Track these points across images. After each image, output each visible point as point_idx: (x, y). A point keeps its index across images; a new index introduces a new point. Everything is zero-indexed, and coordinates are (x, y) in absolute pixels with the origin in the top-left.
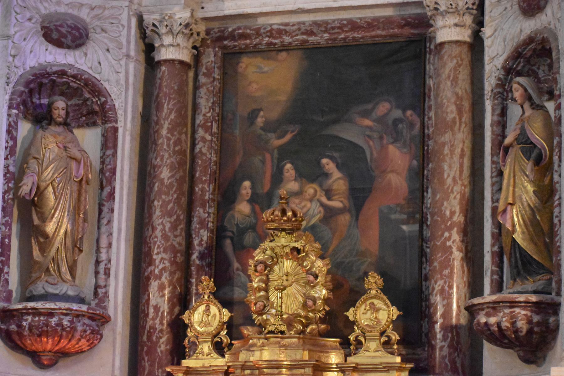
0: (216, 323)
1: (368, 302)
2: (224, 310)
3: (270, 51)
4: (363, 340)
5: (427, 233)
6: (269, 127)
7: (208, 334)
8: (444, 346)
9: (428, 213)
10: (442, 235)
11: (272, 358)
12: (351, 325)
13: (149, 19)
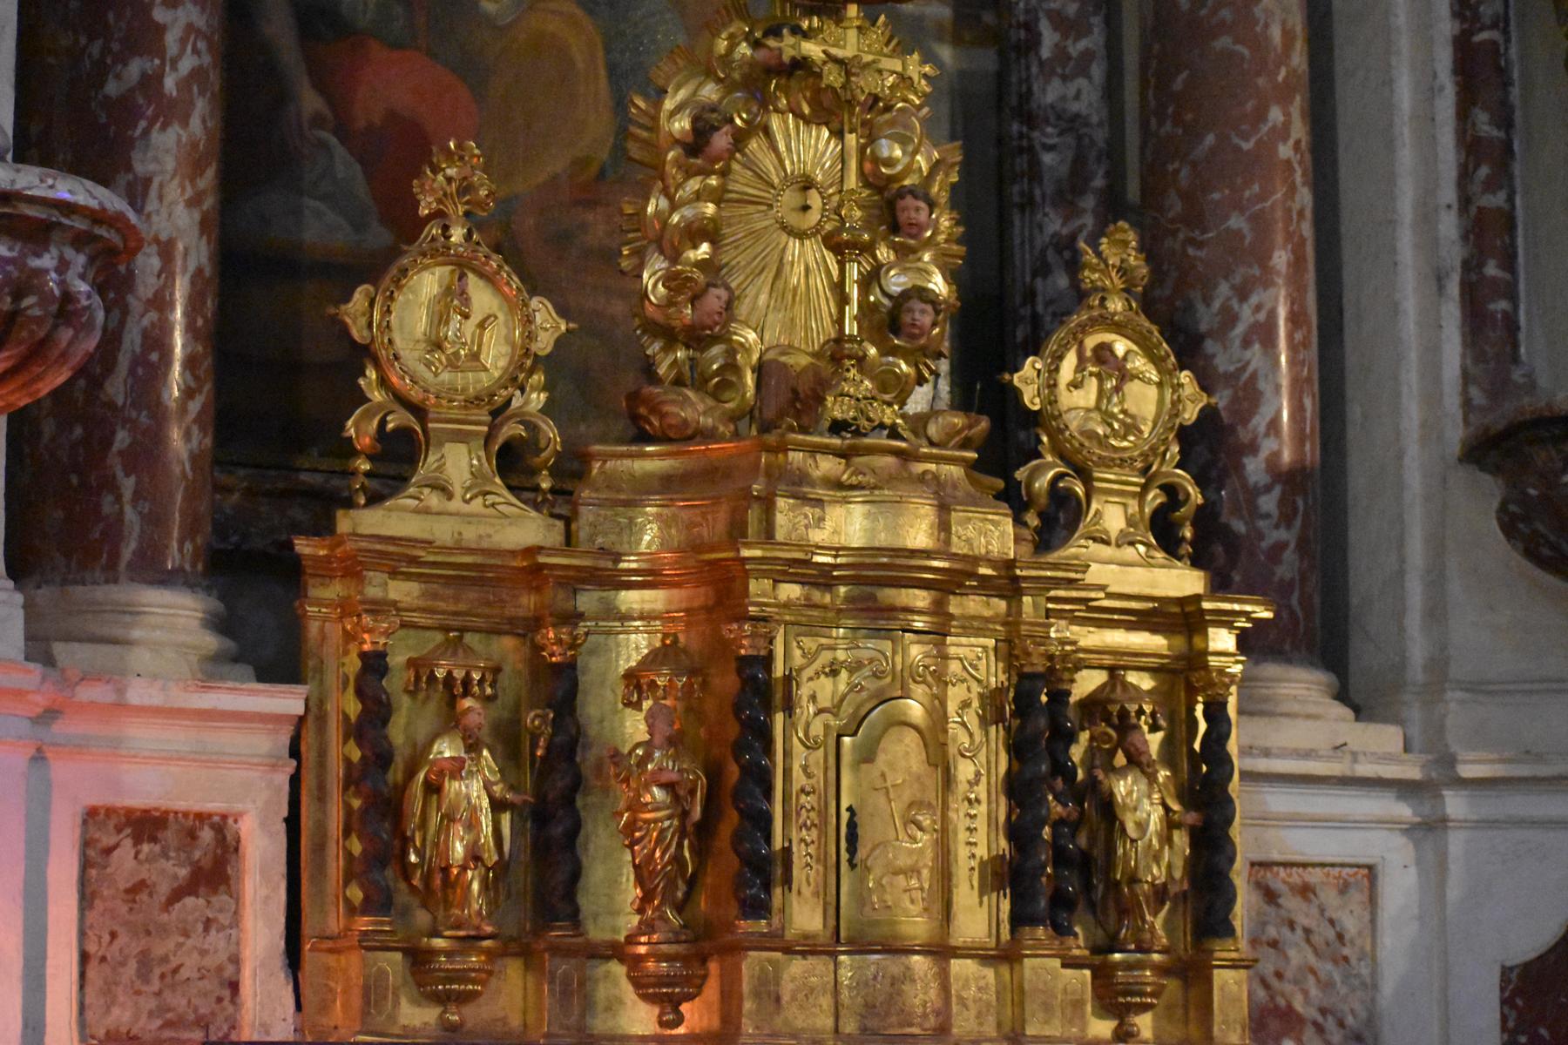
0: (496, 356)
1: (1091, 342)
2: (535, 302)
4: (1079, 490)
7: (475, 401)
8: (1280, 547)
9: (1041, 15)
10: (1261, 115)
11: (883, 540)
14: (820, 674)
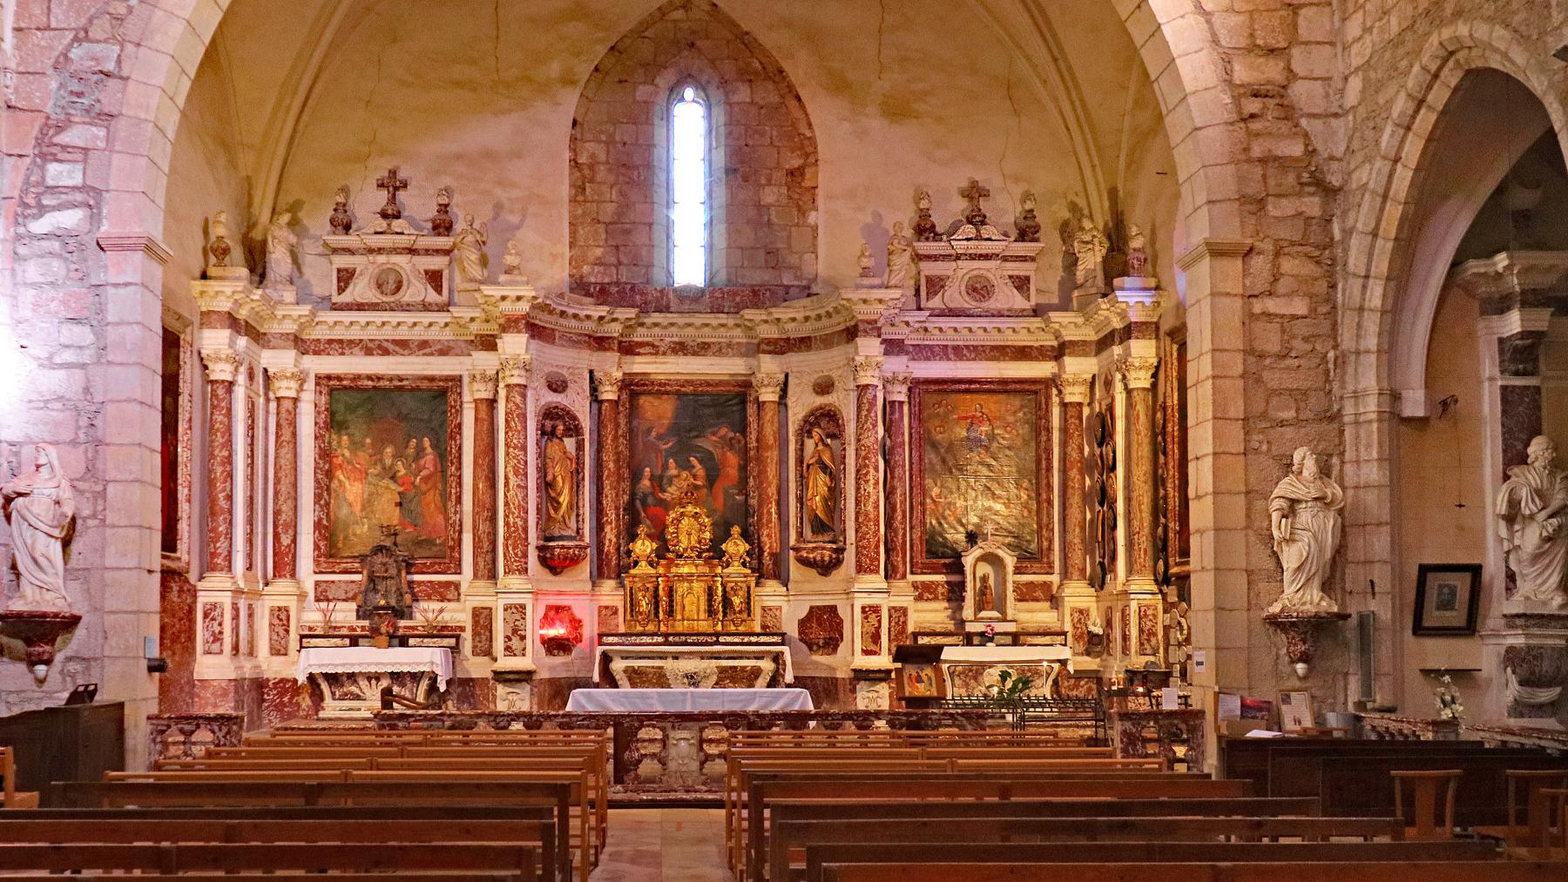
3: (660, 393)
5: (753, 502)
6: (660, 437)
12: (723, 553)
13: (597, 375)
14: (681, 588)
